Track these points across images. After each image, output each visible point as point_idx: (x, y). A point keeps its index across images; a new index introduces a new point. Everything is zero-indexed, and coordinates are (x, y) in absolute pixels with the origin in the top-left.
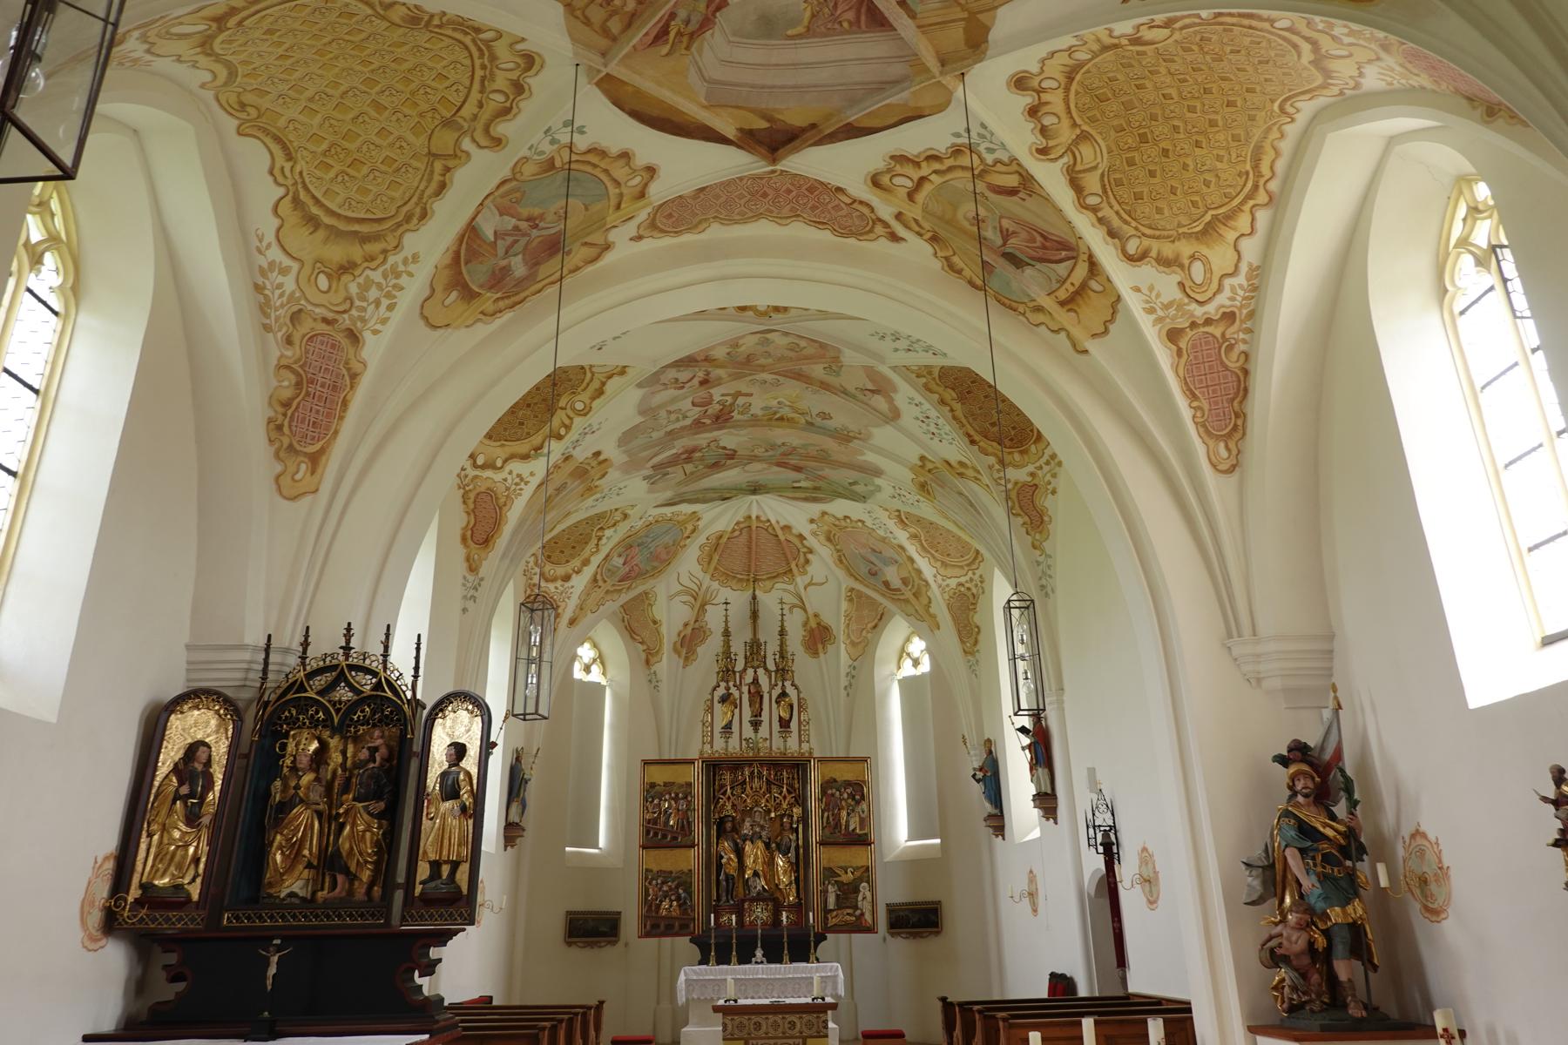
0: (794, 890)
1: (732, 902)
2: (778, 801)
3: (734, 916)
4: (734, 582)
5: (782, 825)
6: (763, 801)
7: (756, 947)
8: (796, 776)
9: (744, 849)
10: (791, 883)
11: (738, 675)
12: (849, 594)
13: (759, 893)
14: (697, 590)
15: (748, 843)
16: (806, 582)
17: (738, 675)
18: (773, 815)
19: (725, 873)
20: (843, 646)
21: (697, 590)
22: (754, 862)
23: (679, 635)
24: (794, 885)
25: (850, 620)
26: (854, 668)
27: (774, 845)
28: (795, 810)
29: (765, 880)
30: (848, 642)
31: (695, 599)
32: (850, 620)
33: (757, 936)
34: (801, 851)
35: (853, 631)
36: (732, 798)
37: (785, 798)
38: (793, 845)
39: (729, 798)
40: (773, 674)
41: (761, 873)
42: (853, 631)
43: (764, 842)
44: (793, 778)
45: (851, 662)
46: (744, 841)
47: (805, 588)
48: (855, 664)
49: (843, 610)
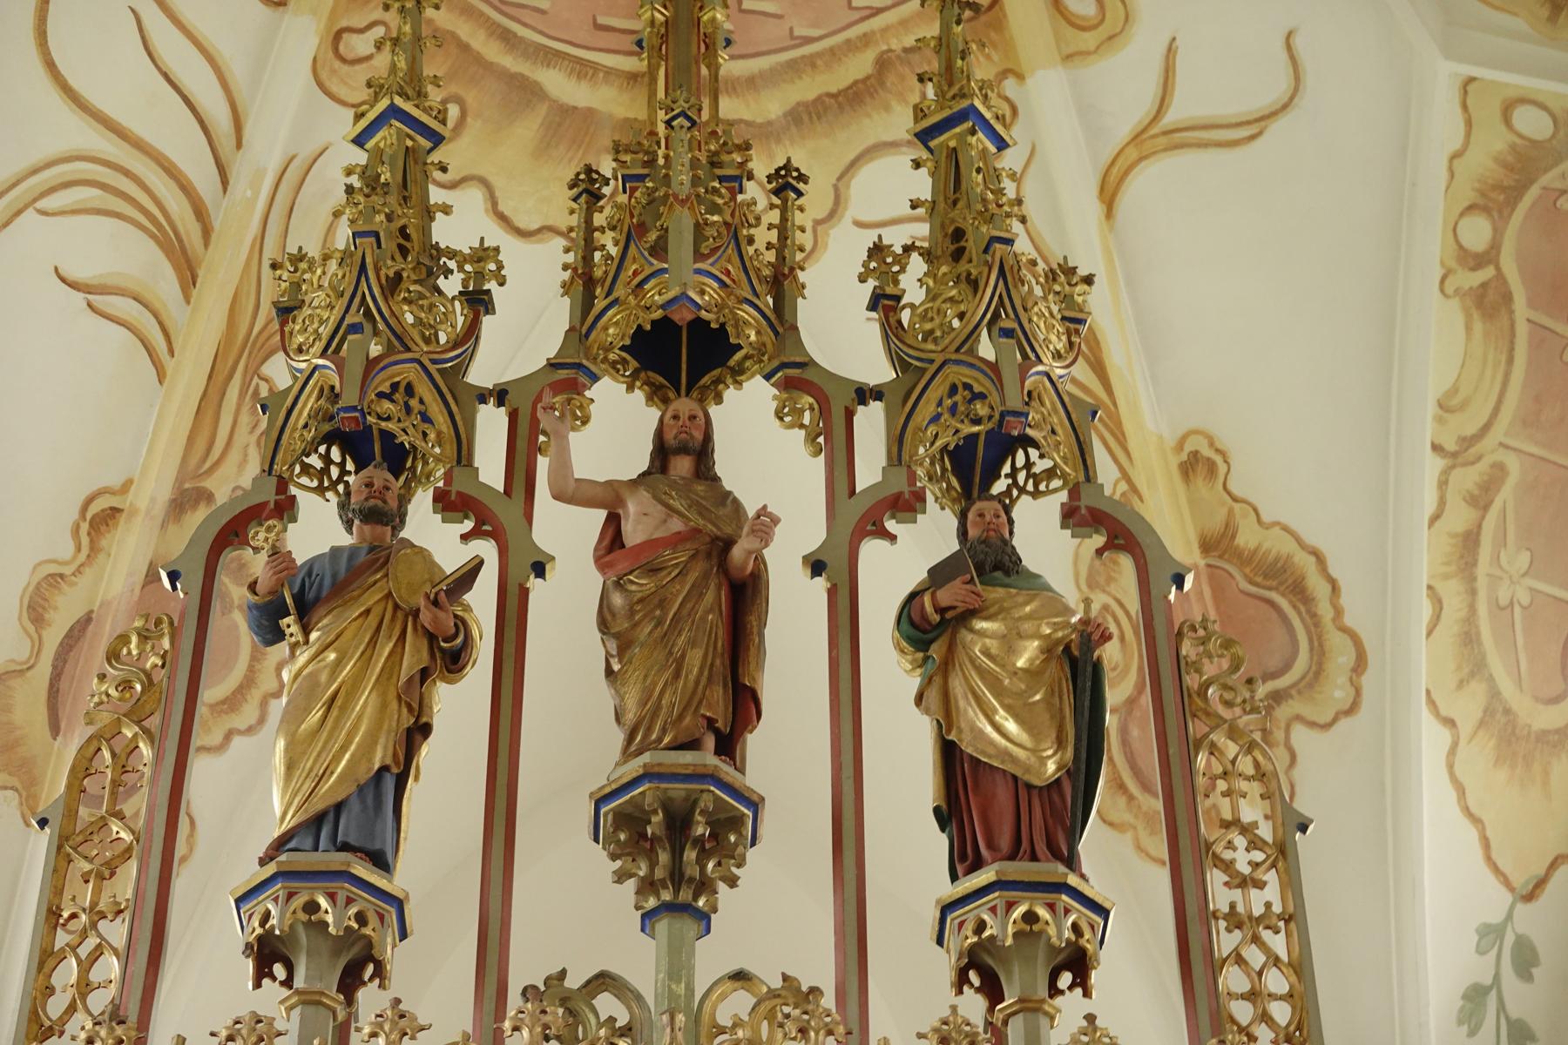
4: (528, 129)
11: (491, 426)
12: (1477, 232)
14: (201, 172)
16: (1124, 123)
17: (491, 426)
20: (1431, 740)
21: (201, 172)
23: (36, 611)
25: (1481, 500)
26: (1525, 960)
30: (1468, 708)
31: (188, 275)
32: (1481, 500)
35: (1503, 610)
40: (871, 423)
42: (1503, 610)
45: (1494, 902)
47: (1109, 194)
49: (1434, 388)
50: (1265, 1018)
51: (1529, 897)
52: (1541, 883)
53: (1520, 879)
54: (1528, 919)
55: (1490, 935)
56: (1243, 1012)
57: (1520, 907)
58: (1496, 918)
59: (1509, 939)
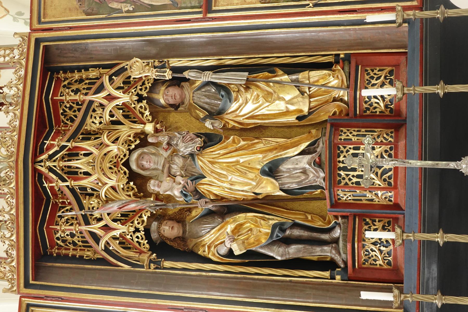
0: (315, 75)
1: (337, 233)
2: (119, 115)
3: (369, 235)
5: (176, 107)
6: (114, 149)
7: (456, 172)
8: (77, 76)
9: (219, 198)
10: (297, 84)
13: (319, 164)
15: (203, 188)
18: (149, 128)
19: (272, 243)
22: (243, 174)
24: (301, 76)
27: (208, 124)
28: (135, 74)
29: (286, 147)
33: (425, 171)
34: (228, 60)
36: (107, 221)
37: (110, 98)
38: (209, 77)
39: (106, 228)
41: (271, 156)
43: (203, 148)
44: (81, 81)
45: (9, 18)
46: (200, 195)
48: (13, 12)
50: (8, 55)
51: (8, 12)
52: (6, 9)
53: (4, 13)
54: (13, 12)
55: (15, 19)
56: (7, 59)
57: (10, 13)
58: (12, 18)
59: (16, 16)
